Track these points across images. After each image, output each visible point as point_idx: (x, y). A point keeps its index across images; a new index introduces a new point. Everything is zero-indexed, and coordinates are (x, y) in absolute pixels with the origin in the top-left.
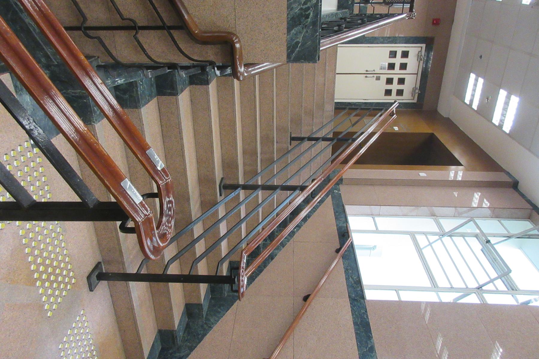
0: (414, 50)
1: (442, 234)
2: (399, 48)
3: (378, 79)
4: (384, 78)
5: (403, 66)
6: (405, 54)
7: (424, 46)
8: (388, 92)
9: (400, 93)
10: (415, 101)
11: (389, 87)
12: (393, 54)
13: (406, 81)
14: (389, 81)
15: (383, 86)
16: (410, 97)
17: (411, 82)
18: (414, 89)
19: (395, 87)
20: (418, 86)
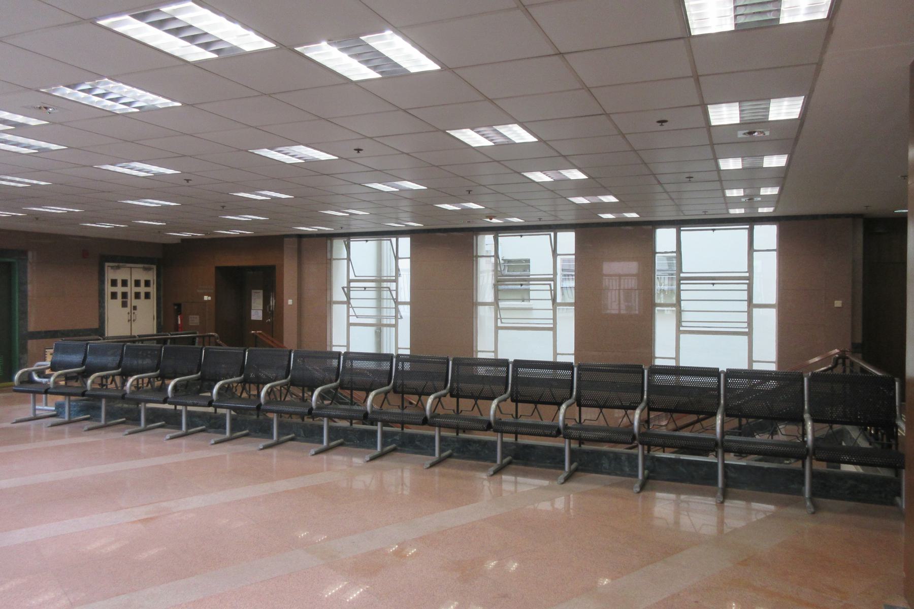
0: (110, 275)
1: (348, 303)
2: (109, 289)
3: (135, 308)
4: (135, 302)
5: (124, 283)
6: (114, 283)
7: (107, 264)
8: (147, 296)
9: (147, 283)
10: (155, 267)
11: (143, 295)
12: (114, 295)
13: (138, 278)
14: (137, 296)
15: (141, 303)
16: (150, 273)
17: (140, 274)
18: (145, 269)
19: (142, 289)
20: (141, 266)
